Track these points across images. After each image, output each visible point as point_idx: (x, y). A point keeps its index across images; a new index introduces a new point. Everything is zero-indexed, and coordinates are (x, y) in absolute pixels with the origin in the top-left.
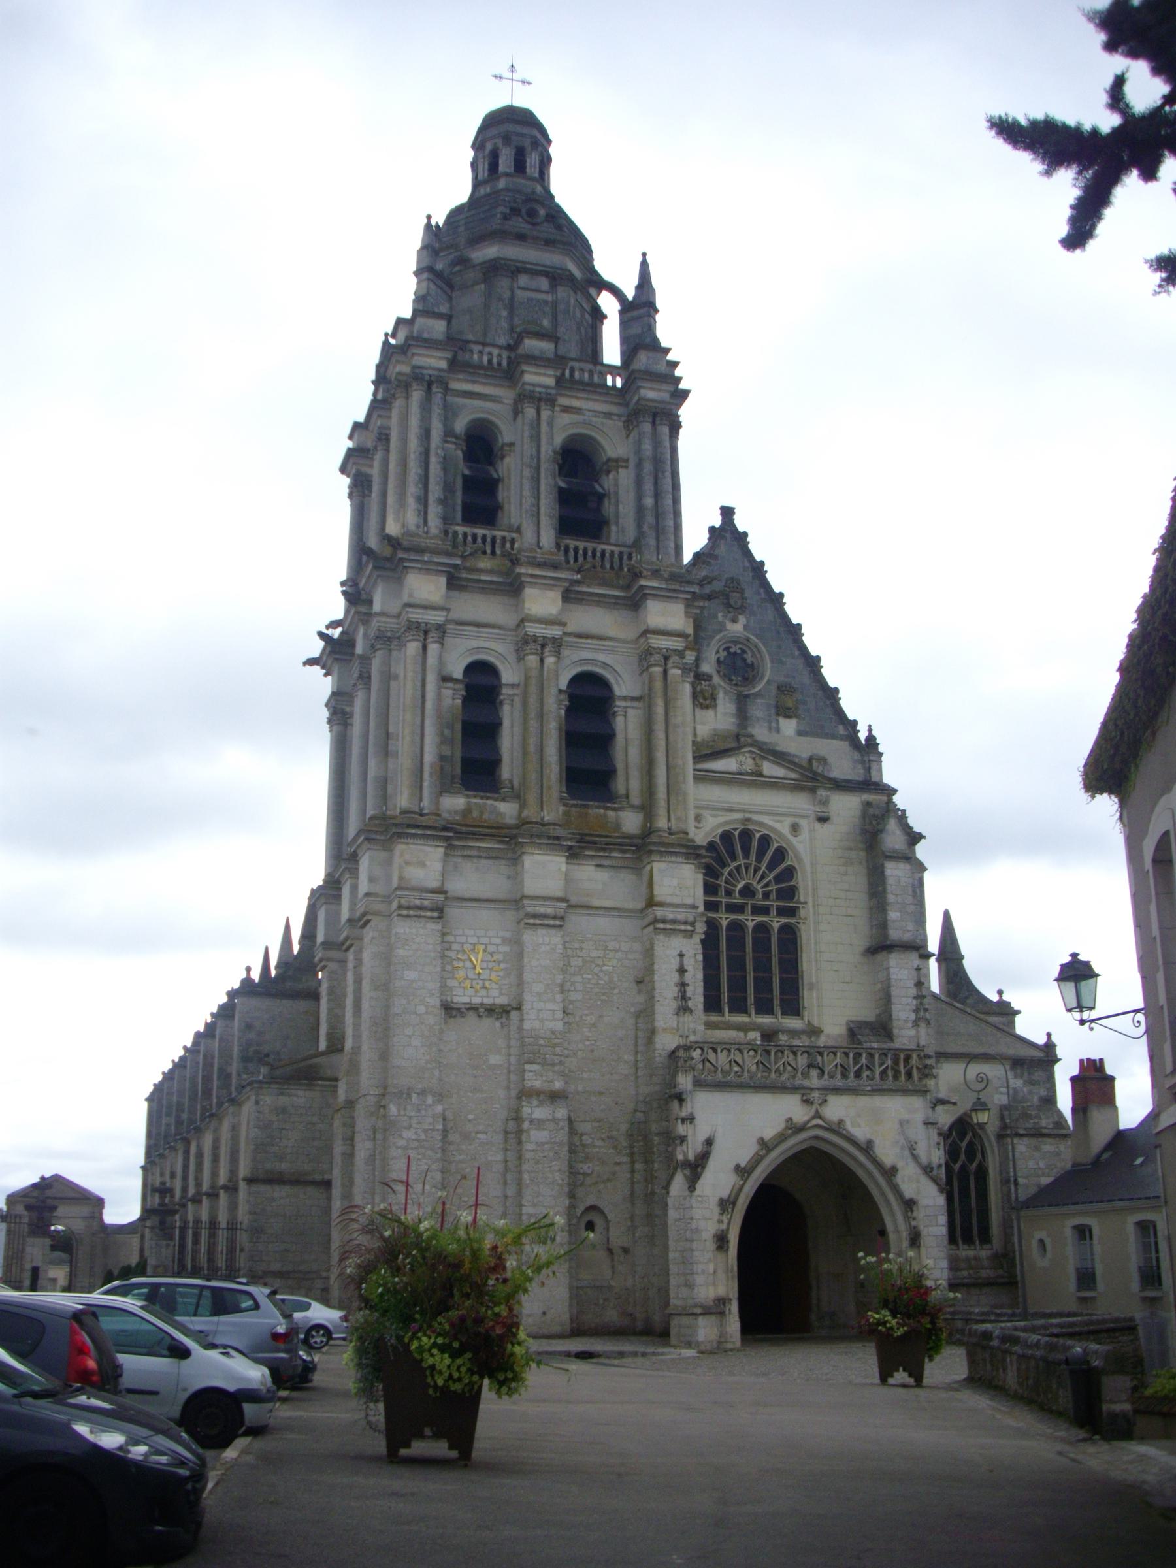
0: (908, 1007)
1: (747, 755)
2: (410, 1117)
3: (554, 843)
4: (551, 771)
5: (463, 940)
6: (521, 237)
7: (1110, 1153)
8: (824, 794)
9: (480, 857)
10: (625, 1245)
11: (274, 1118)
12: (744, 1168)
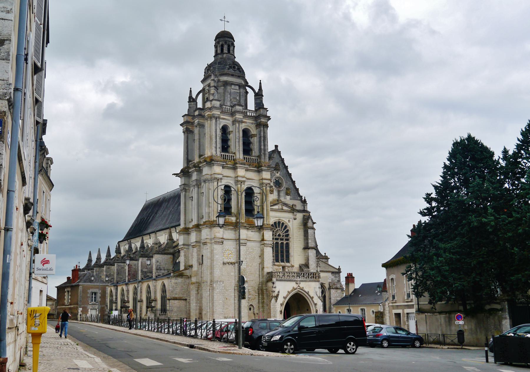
3: (245, 227)
5: (225, 248)
6: (232, 75)
11: (174, 285)
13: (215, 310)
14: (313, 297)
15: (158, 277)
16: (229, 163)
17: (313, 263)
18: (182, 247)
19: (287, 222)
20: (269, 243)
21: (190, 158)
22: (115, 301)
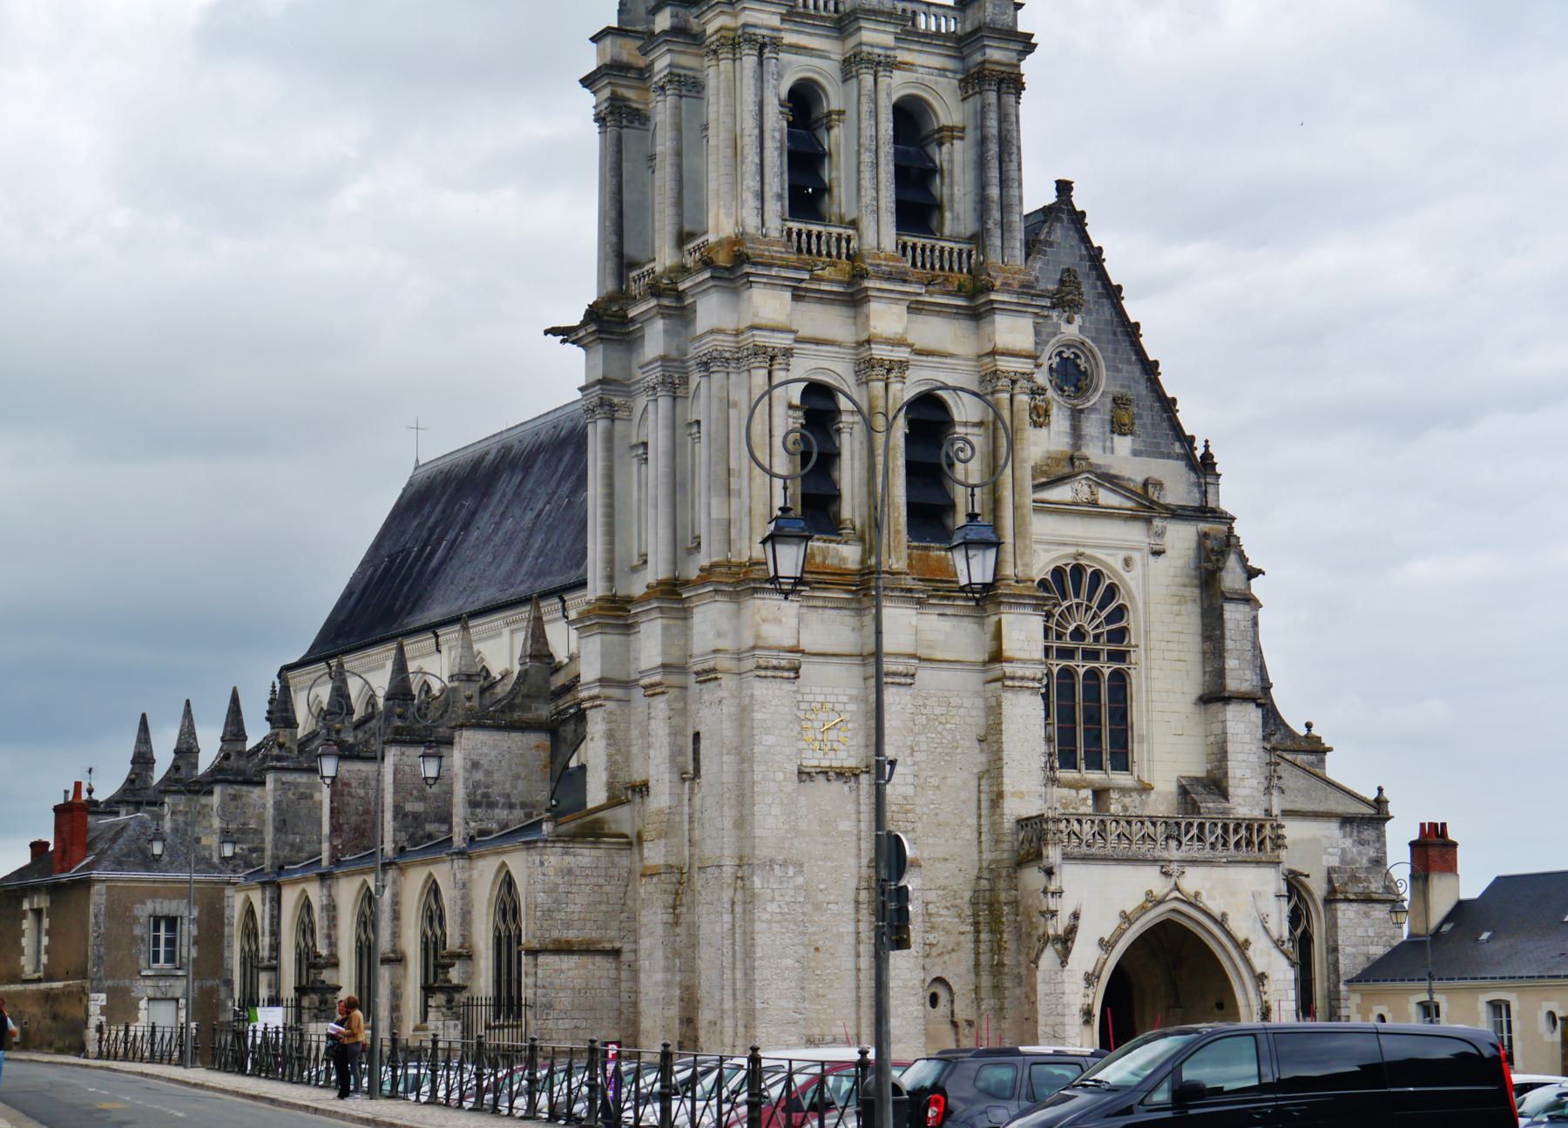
0: (1244, 764)
1: (1084, 482)
2: (773, 890)
3: (907, 595)
4: (899, 514)
5: (810, 697)
7: (1451, 925)
8: (1160, 524)
9: (826, 607)
10: (970, 1018)
11: (560, 881)
12: (1108, 942)
13: (759, 1006)
14: (1247, 942)
15: (477, 843)
16: (826, 273)
17: (1248, 773)
18: (595, 691)
19: (1118, 565)
20: (1029, 673)
21: (630, 249)
22: (270, 958)
